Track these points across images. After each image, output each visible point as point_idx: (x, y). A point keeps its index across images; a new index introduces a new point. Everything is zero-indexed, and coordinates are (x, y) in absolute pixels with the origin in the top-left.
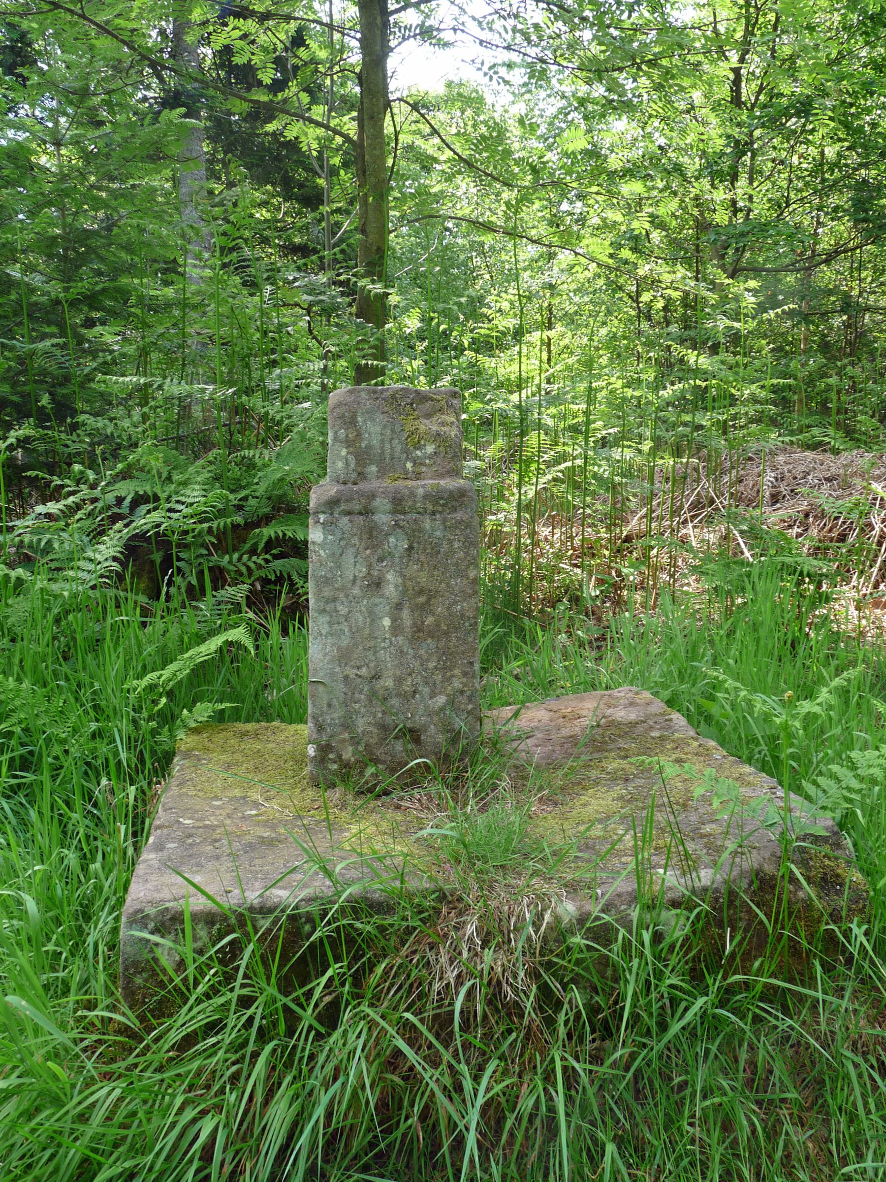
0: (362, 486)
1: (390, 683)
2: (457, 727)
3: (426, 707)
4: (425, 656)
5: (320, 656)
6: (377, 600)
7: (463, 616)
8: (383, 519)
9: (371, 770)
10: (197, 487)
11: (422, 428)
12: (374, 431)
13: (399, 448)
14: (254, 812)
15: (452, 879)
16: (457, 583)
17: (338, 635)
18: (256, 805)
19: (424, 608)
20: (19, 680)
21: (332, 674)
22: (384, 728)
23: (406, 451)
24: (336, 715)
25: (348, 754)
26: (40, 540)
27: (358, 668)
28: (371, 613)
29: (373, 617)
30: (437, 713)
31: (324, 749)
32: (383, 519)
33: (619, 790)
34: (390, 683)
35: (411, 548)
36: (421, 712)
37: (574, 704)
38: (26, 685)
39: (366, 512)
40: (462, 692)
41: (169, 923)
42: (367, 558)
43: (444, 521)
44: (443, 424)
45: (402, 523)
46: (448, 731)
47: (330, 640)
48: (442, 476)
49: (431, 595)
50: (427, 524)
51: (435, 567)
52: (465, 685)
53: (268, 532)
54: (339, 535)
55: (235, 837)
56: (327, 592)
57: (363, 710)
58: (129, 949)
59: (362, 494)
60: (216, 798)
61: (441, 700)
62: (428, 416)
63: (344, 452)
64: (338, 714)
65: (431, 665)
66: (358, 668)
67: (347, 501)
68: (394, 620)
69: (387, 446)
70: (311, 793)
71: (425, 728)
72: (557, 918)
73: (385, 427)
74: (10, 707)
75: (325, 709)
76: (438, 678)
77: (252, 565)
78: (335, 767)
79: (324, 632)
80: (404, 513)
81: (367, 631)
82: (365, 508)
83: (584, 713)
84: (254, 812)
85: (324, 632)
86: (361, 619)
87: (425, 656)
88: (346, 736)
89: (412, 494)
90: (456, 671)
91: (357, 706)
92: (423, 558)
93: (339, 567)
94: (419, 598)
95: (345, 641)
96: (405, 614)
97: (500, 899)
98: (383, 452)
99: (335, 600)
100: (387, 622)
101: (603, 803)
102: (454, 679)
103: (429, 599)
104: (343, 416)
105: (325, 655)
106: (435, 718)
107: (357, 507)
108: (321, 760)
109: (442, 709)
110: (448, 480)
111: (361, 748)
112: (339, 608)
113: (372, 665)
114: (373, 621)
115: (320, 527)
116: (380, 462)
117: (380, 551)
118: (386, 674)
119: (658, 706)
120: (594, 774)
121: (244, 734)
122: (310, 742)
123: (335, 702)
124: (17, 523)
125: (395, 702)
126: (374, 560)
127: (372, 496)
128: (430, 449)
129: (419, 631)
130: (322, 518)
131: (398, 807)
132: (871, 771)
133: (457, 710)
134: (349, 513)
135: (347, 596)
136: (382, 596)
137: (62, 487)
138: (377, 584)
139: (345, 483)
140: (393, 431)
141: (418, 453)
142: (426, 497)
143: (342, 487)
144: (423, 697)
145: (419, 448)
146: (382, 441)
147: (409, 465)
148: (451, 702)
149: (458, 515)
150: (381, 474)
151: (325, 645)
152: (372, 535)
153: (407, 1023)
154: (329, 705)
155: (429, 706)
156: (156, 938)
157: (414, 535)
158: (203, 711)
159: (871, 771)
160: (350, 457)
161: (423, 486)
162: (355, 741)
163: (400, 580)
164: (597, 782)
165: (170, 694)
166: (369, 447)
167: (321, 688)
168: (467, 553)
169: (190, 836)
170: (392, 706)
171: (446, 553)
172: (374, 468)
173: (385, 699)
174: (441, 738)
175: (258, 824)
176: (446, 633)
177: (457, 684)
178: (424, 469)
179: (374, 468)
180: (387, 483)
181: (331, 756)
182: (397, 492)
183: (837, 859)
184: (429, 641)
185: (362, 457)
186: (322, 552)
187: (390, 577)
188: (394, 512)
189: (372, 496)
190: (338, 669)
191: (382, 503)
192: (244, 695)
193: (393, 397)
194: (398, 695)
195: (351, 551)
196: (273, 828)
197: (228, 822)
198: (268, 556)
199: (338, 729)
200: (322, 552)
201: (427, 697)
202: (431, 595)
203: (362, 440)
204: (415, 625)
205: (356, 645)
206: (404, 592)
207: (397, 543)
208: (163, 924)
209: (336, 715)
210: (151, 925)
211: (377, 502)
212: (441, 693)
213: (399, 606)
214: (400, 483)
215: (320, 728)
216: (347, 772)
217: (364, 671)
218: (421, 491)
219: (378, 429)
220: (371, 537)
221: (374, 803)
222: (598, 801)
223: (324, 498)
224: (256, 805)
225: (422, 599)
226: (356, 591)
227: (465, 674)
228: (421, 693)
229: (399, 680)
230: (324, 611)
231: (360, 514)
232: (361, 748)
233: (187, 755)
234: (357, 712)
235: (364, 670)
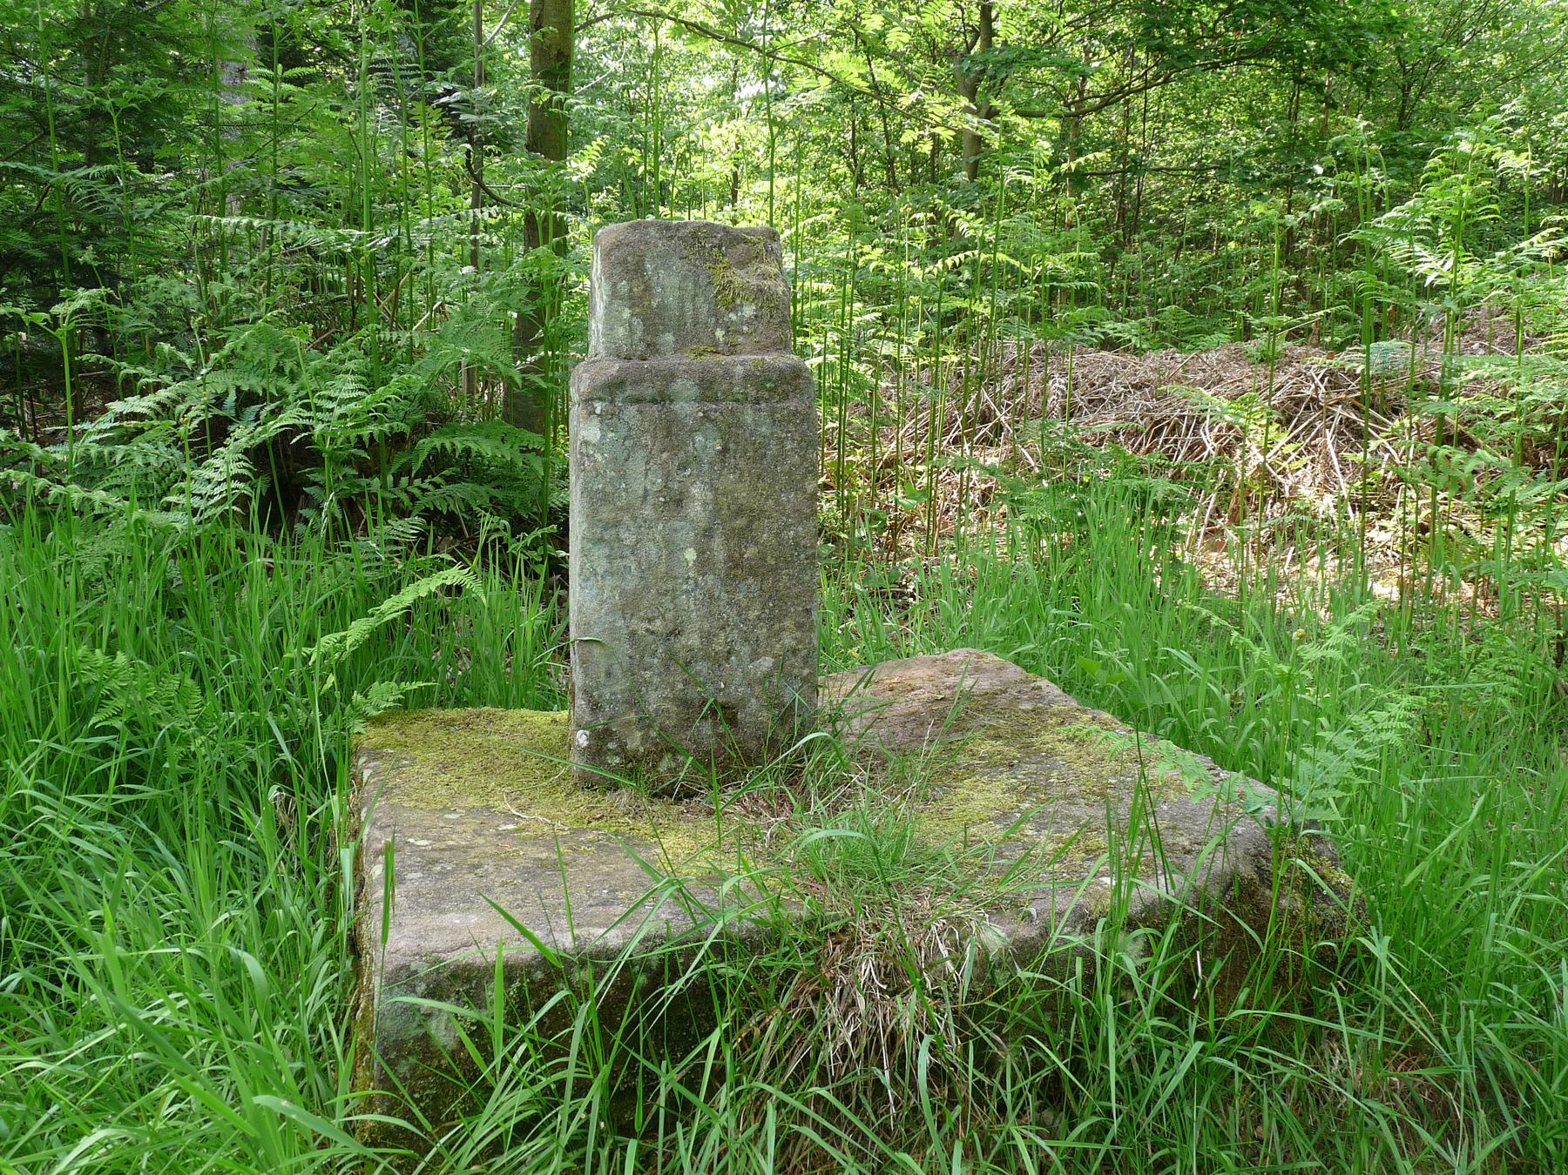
0: (653, 362)
1: (694, 640)
2: (787, 700)
3: (745, 673)
4: (745, 603)
5: (594, 605)
6: (678, 524)
7: (797, 544)
8: (686, 408)
9: (666, 763)
10: (349, 377)
11: (737, 281)
12: (669, 283)
13: (704, 309)
14: (511, 827)
15: (836, 906)
16: (790, 499)
17: (622, 573)
18: (510, 817)
19: (743, 535)
20: (111, 652)
21: (613, 630)
22: (685, 703)
23: (715, 313)
24: (617, 688)
25: (635, 742)
26: (112, 454)
27: (650, 621)
28: (668, 542)
29: (671, 547)
30: (761, 683)
31: (601, 737)
32: (686, 408)
33: (1006, 779)
34: (694, 640)
35: (725, 450)
36: (737, 680)
37: (898, 672)
38: (121, 658)
39: (663, 399)
40: (794, 652)
41: (463, 982)
42: (663, 465)
43: (773, 412)
44: (764, 276)
45: (713, 415)
46: (776, 706)
47: (609, 582)
48: (765, 349)
49: (754, 516)
50: (748, 417)
51: (759, 477)
52: (800, 642)
53: (427, 444)
54: (624, 432)
55: (483, 864)
56: (606, 514)
57: (656, 680)
58: (388, 1023)
59: (656, 373)
60: (445, 809)
61: (767, 663)
62: (742, 264)
63: (626, 314)
64: (620, 686)
65: (753, 614)
66: (650, 621)
67: (635, 383)
68: (700, 552)
69: (689, 305)
70: (582, 798)
71: (743, 703)
72: (983, 952)
73: (685, 277)
74: (104, 692)
75: (602, 679)
76: (762, 632)
77: (417, 492)
78: (617, 760)
79: (600, 571)
80: (716, 401)
81: (662, 568)
82: (661, 393)
83: (918, 683)
84: (511, 827)
85: (600, 571)
86: (654, 551)
87: (745, 603)
88: (632, 716)
89: (728, 374)
90: (788, 623)
91: (648, 674)
92: (742, 464)
93: (623, 477)
94: (737, 521)
95: (631, 583)
96: (717, 543)
97: (896, 928)
98: (682, 314)
99: (617, 524)
100: (691, 555)
101: (992, 796)
102: (785, 634)
103: (751, 522)
104: (625, 261)
105: (602, 603)
106: (758, 689)
107: (650, 393)
108: (596, 752)
109: (768, 675)
110: (775, 355)
111: (653, 734)
112: (624, 536)
113: (669, 615)
114: (671, 553)
115: (596, 421)
116: (679, 329)
117: (682, 455)
118: (689, 628)
119: (1014, 672)
120: (963, 759)
121: (450, 723)
122: (579, 727)
123: (617, 670)
124: (86, 426)
125: (701, 667)
126: (673, 467)
127: (671, 376)
128: (749, 311)
129: (736, 566)
130: (599, 407)
131: (710, 813)
132: (1384, 736)
133: (788, 676)
134: (638, 401)
135: (634, 519)
136: (685, 518)
137: (137, 377)
138: (676, 502)
139: (628, 358)
140: (696, 284)
141: (733, 316)
142: (746, 377)
143: (627, 364)
144: (740, 659)
145: (734, 310)
146: (681, 299)
147: (719, 333)
148: (780, 665)
149: (792, 404)
150: (681, 345)
151: (602, 588)
152: (671, 432)
153: (819, 1098)
154: (608, 674)
155: (747, 675)
156: (428, 1003)
157: (730, 433)
158: (384, 694)
159: (1384, 736)
160: (636, 321)
161: (742, 363)
162: (644, 723)
163: (710, 496)
164: (970, 770)
165: (339, 669)
166: (663, 307)
167: (596, 650)
168: (803, 458)
169: (435, 862)
170: (698, 673)
171: (774, 457)
172: (669, 337)
173: (688, 664)
174: (765, 716)
175: (524, 841)
176: (774, 570)
177: (788, 641)
178: (741, 339)
179: (669, 337)
180: (688, 358)
181: (611, 746)
182: (705, 370)
183: (1319, 854)
184: (751, 580)
185: (653, 321)
186: (598, 457)
187: (695, 490)
188: (703, 399)
189: (671, 376)
190: (620, 623)
191: (684, 387)
192: (438, 674)
193: (694, 235)
194: (706, 657)
195: (640, 455)
196: (549, 847)
197: (481, 840)
198: (437, 479)
199: (620, 708)
200: (598, 457)
201: (746, 659)
202: (754, 516)
203: (652, 296)
204: (730, 558)
205: (647, 588)
206: (717, 512)
207: (706, 443)
208: (438, 984)
209: (617, 688)
210: (422, 988)
211: (678, 385)
212: (765, 654)
213: (708, 533)
214: (708, 359)
215: (595, 707)
216: (632, 765)
217: (658, 625)
218: (739, 370)
219: (675, 281)
220: (669, 434)
221: (675, 809)
222: (983, 796)
223: (601, 379)
224: (510, 817)
225: (740, 522)
226: (648, 511)
227: (799, 626)
228: (738, 654)
229: (708, 637)
230: (601, 540)
231: (654, 401)
232: (653, 734)
233: (375, 754)
234: (648, 683)
235: (658, 623)
